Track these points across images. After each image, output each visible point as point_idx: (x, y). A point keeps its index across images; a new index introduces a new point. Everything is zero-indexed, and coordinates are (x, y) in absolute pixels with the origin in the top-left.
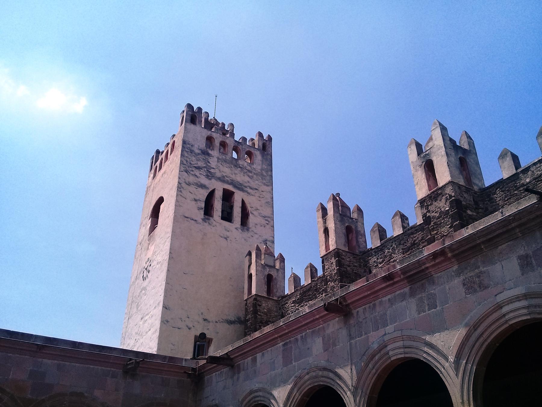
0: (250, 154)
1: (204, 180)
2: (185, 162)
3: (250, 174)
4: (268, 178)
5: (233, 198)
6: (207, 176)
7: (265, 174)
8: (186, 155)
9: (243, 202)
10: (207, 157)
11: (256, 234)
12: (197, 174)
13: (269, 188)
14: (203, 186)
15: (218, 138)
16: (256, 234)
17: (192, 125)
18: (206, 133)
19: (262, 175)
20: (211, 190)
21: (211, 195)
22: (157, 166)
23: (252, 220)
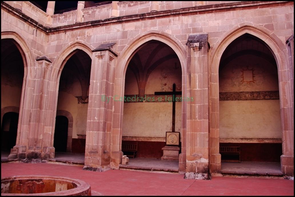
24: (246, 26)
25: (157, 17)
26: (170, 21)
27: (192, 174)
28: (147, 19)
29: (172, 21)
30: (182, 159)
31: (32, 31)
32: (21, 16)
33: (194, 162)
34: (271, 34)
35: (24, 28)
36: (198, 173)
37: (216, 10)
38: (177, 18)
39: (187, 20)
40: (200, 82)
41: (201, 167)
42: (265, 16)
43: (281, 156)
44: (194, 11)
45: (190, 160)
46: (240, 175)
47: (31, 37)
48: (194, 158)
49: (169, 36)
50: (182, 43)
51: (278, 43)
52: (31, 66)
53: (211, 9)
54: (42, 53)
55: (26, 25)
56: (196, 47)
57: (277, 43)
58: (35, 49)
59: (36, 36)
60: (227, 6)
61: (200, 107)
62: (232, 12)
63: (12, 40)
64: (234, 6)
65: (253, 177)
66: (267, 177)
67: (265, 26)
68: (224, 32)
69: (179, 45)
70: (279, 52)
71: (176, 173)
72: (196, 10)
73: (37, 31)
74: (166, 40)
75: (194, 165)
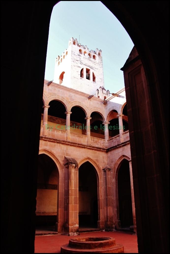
0: (94, 57)
1: (80, 65)
2: (73, 58)
3: (95, 64)
4: (101, 65)
5: (89, 72)
6: (81, 63)
7: (100, 63)
8: (73, 55)
9: (93, 73)
10: (80, 57)
11: (98, 84)
12: (77, 63)
13: (102, 69)
14: (79, 67)
15: (83, 50)
16: (98, 84)
17: (74, 45)
18: (79, 48)
19: (99, 64)
20: (82, 68)
21: (82, 70)
22: (59, 62)
23: (96, 79)
24: (89, 158)
25: (48, 141)
26: (55, 145)
27: (72, 233)
28: (42, 140)
29: (56, 146)
30: (59, 226)
33: (73, 226)
34: (98, 164)
36: (75, 232)
37: (77, 146)
38: (59, 144)
39: (64, 147)
40: (75, 185)
41: (76, 229)
42: (96, 155)
43: (98, 221)
44: (68, 144)
45: (71, 226)
46: (85, 232)
48: (73, 224)
49: (54, 154)
50: (61, 160)
51: (99, 169)
53: (76, 145)
56: (74, 166)
57: (99, 169)
60: (83, 146)
61: (75, 198)
62: (83, 149)
64: (85, 147)
65: (90, 232)
66: (95, 232)
67: (96, 160)
68: (80, 158)
69: (59, 161)
70: (99, 173)
71: (57, 235)
72: (69, 144)
74: (52, 156)
75: (73, 228)
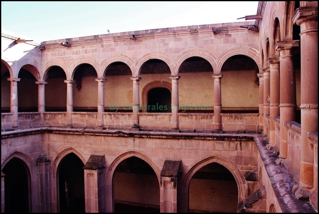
31: (235, 147)
32: (215, 139)
35: (223, 147)
47: (234, 154)
52: (241, 184)
54: (253, 166)
55: (226, 143)
58: (242, 165)
59: (241, 149)
63: (214, 163)
73: (241, 144)
